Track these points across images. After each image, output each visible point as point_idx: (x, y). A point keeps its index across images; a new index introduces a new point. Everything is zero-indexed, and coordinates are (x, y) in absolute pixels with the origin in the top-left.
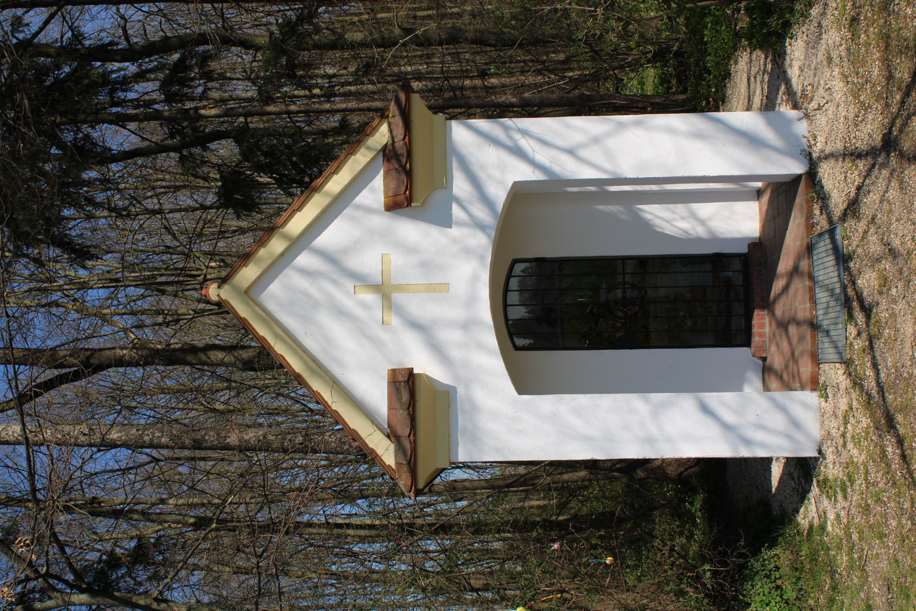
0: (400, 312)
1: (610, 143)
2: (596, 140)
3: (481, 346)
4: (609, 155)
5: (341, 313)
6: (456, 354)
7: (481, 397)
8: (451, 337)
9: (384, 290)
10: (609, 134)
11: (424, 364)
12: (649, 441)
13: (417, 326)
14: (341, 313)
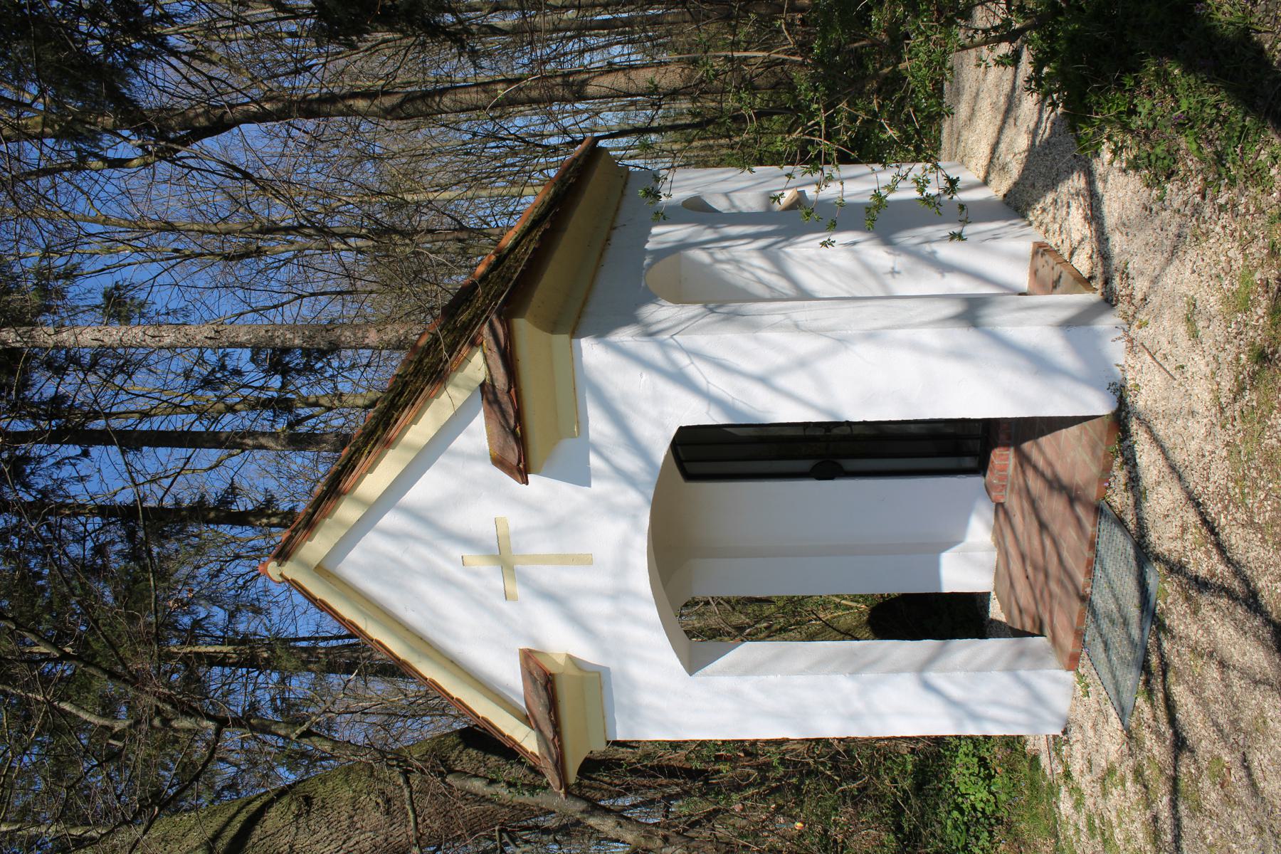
0: (526, 581)
1: (824, 367)
2: (802, 363)
3: (636, 620)
4: (821, 383)
5: (446, 582)
6: (603, 627)
7: (637, 671)
8: (596, 609)
9: (503, 556)
10: (824, 354)
11: (562, 643)
12: (854, 717)
13: (548, 596)
14: (446, 582)
